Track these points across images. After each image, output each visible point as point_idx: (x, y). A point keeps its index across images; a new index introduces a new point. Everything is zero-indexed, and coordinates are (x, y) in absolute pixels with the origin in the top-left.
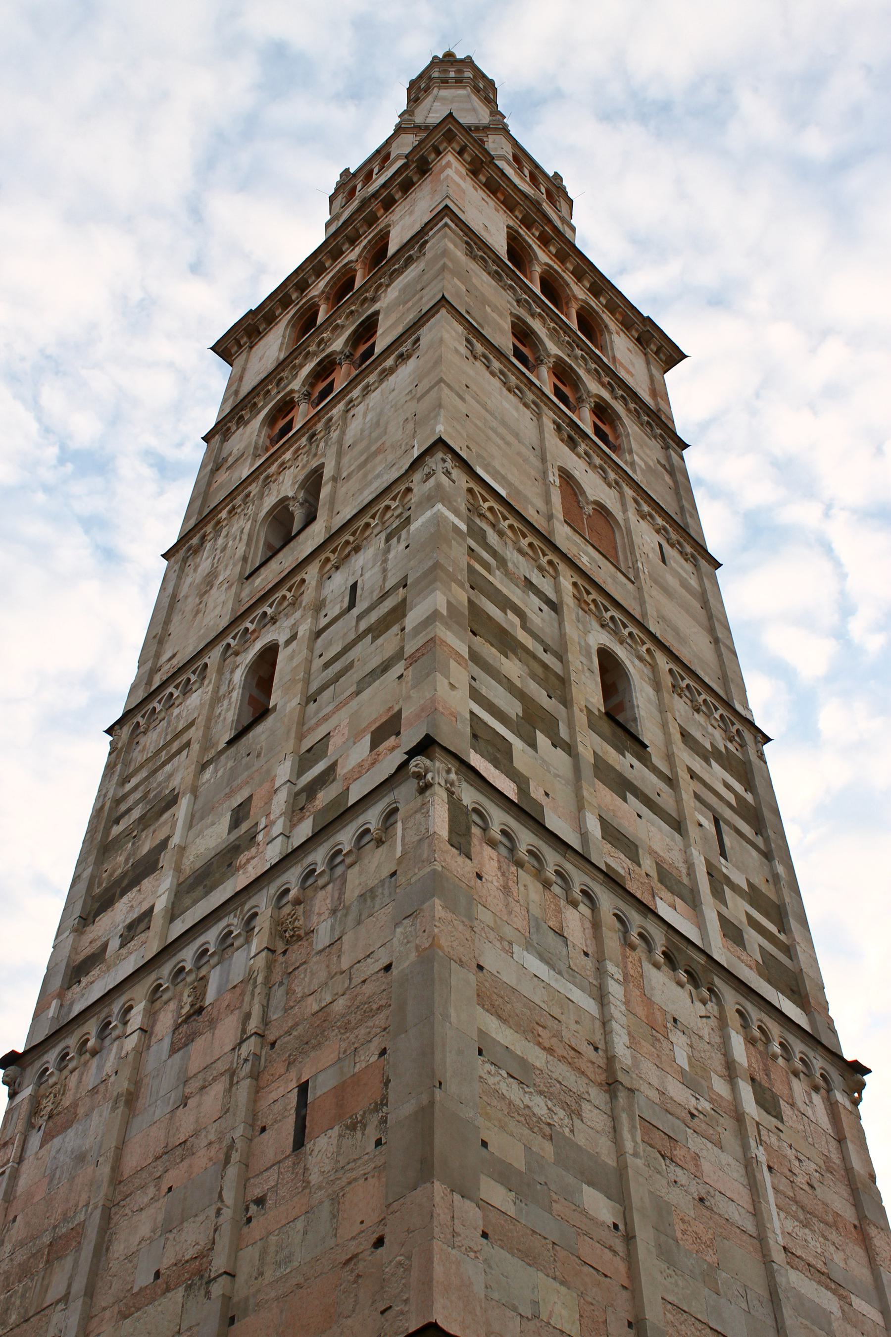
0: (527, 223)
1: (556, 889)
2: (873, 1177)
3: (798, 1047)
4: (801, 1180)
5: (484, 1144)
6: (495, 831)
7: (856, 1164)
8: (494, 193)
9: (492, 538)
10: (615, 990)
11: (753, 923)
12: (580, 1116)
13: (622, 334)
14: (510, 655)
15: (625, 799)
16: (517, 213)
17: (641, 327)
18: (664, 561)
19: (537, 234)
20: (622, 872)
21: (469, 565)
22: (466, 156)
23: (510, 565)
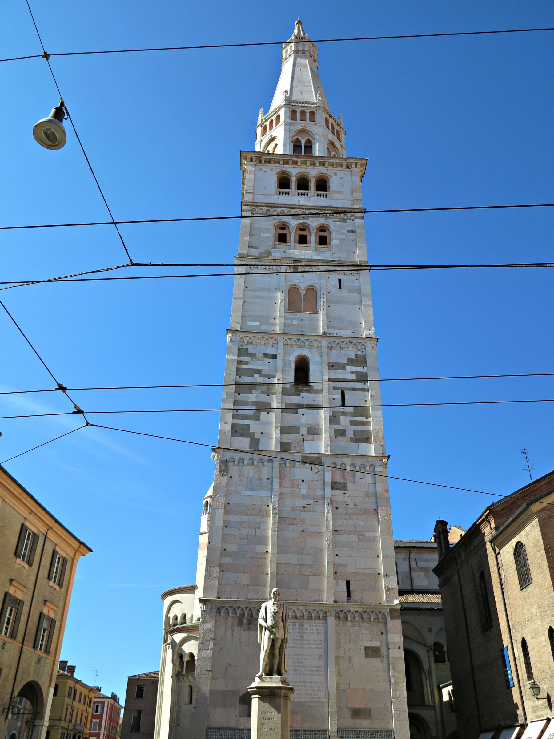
0: (286, 163)
1: (260, 464)
2: (387, 491)
3: (359, 462)
4: (351, 505)
5: (225, 550)
6: (236, 462)
7: (380, 488)
8: (270, 162)
9: (251, 349)
10: (276, 485)
11: (353, 423)
12: (259, 528)
13: (338, 172)
14: (253, 391)
15: (297, 413)
16: (281, 163)
17: (345, 162)
18: (340, 287)
19: (291, 163)
20: (290, 441)
21: (238, 369)
22: (254, 160)
23: (257, 355)
